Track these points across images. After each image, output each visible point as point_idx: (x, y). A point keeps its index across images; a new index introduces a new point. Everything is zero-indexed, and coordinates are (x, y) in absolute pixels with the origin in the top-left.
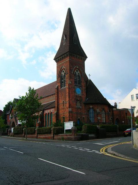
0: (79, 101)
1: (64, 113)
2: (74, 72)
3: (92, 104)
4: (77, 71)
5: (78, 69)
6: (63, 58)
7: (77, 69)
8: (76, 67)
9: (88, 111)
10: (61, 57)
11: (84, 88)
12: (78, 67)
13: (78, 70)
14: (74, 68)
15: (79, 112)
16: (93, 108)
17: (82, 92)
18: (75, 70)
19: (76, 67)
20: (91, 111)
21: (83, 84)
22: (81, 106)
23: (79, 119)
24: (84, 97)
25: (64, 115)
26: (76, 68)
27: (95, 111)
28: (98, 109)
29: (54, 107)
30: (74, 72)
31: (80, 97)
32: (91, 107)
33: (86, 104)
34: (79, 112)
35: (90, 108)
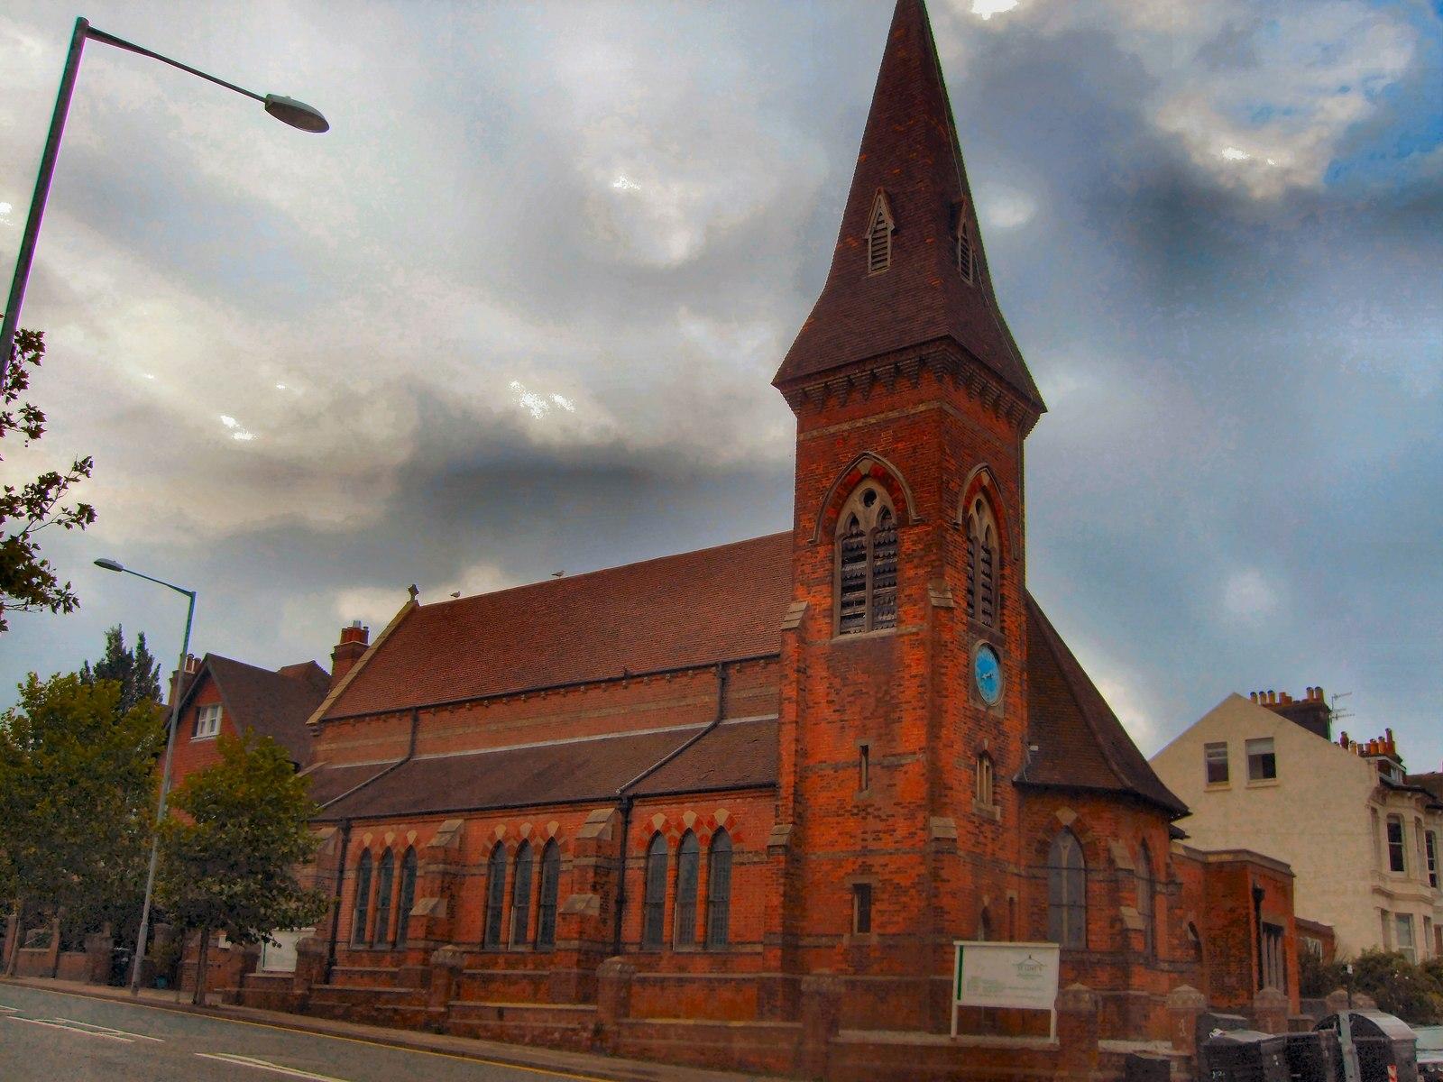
0: (986, 763)
1: (865, 851)
2: (966, 510)
3: (1074, 794)
4: (979, 504)
5: (984, 490)
6: (874, 377)
7: (980, 496)
8: (978, 478)
9: (1043, 848)
10: (856, 373)
11: (1017, 656)
12: (986, 480)
13: (984, 501)
14: (966, 488)
15: (989, 850)
16: (1075, 831)
17: (1008, 679)
18: (968, 502)
19: (978, 478)
20: (1065, 850)
21: (1015, 621)
22: (995, 802)
23: (985, 911)
24: (1016, 727)
25: (866, 869)
26: (977, 486)
27: (1089, 851)
28: (1116, 836)
29: (770, 788)
30: (966, 510)
31: (998, 723)
32: (1067, 816)
33: (1021, 787)
34: (989, 850)
35: (1054, 828)
